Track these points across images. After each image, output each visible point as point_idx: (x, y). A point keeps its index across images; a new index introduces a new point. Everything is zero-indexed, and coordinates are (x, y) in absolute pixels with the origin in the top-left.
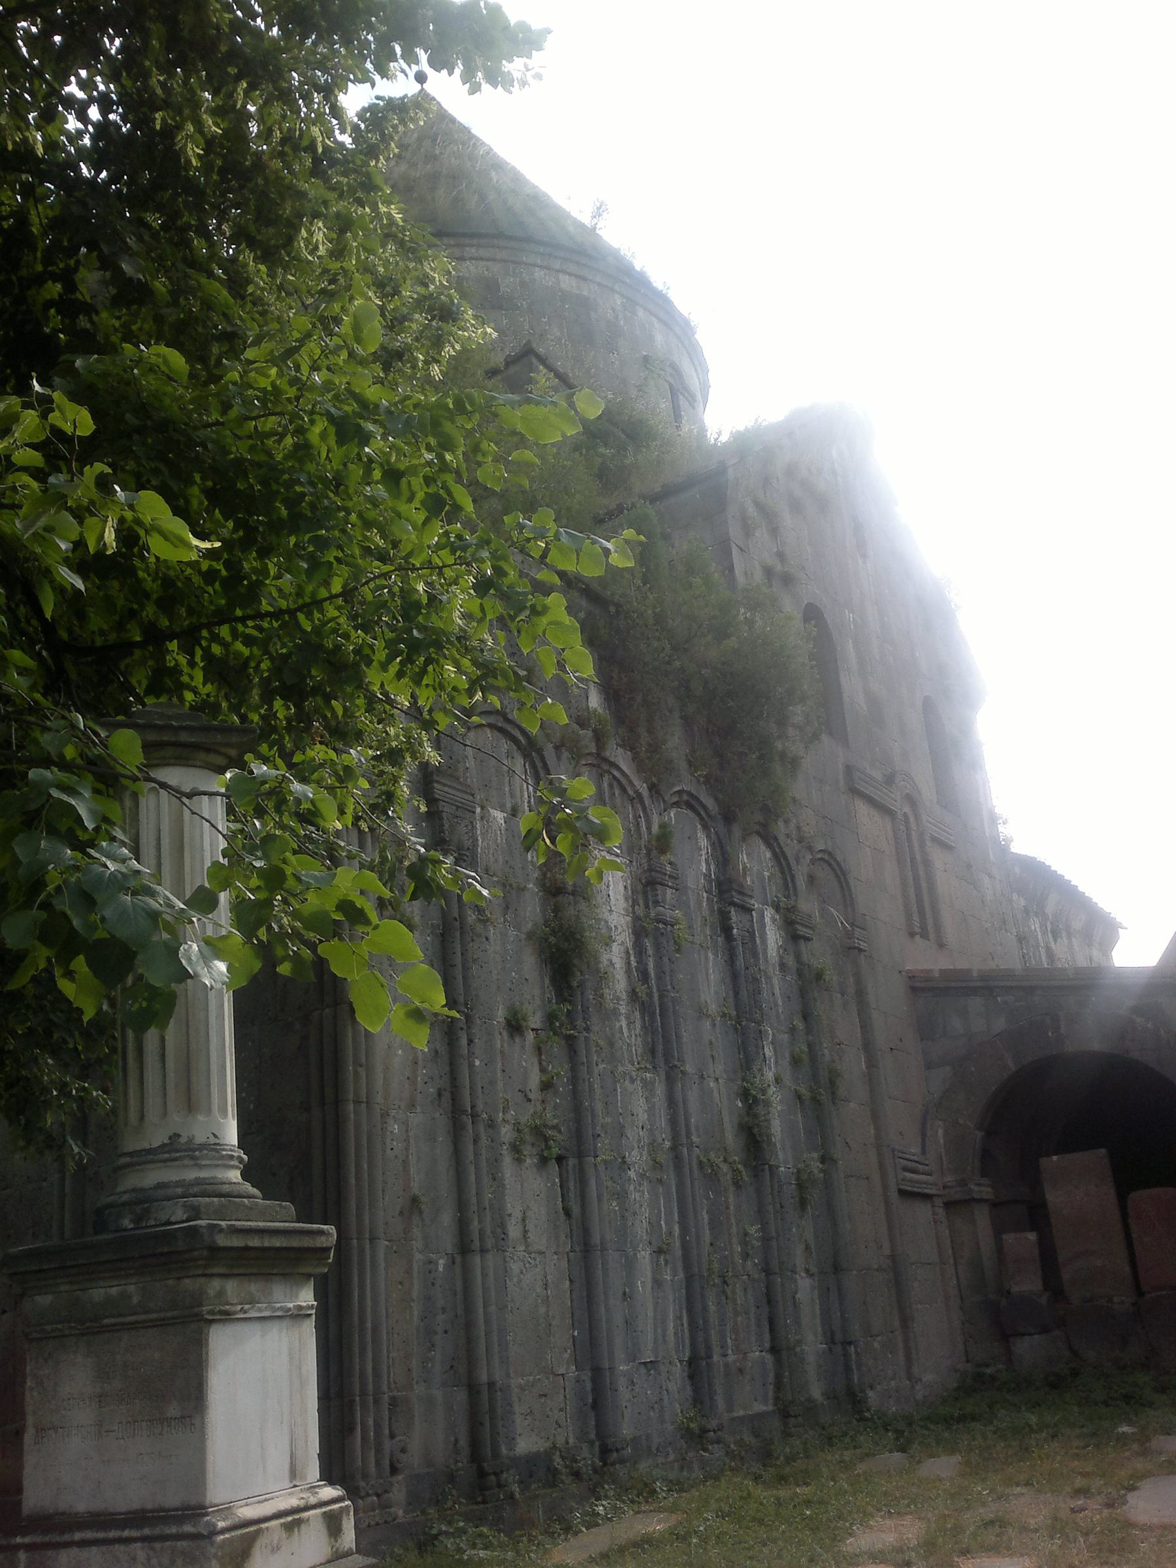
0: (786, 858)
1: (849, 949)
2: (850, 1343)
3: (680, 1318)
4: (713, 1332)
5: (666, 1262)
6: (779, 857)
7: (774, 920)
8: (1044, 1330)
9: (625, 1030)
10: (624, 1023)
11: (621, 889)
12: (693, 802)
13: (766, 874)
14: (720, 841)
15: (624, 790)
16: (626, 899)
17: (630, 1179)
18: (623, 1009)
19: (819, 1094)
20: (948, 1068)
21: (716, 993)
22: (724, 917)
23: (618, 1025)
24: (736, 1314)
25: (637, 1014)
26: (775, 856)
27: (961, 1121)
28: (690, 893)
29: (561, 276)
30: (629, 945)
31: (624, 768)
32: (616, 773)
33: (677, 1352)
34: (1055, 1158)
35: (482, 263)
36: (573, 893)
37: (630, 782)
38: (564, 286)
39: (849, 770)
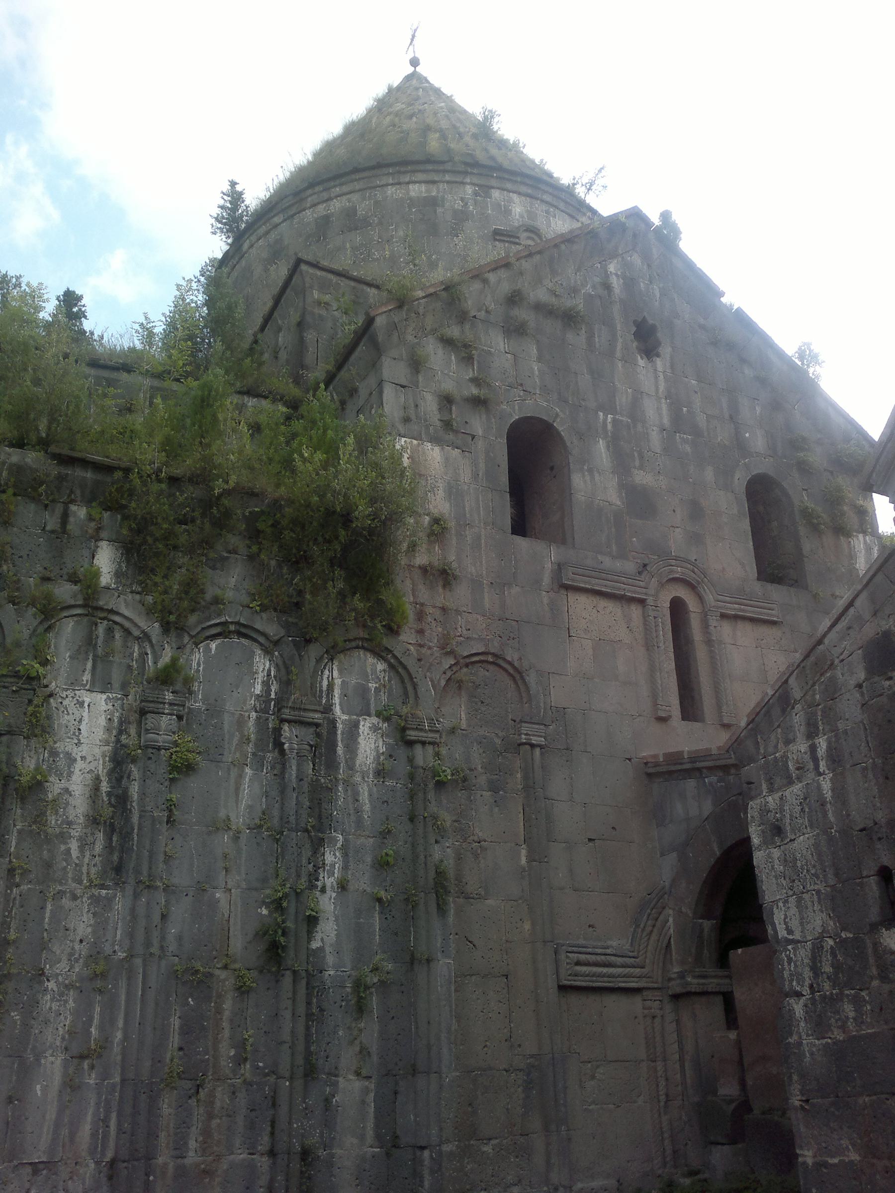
0: (405, 668)
1: (519, 745)
2: (423, 1148)
3: (106, 1121)
4: (163, 1135)
5: (92, 1067)
6: (397, 667)
7: (375, 729)
8: (733, 1141)
9: (75, 853)
10: (74, 846)
11: (102, 721)
12: (243, 630)
13: (372, 686)
14: (284, 662)
15: (127, 632)
16: (108, 730)
17: (46, 990)
18: (76, 832)
19: (416, 894)
20: (675, 855)
21: (250, 807)
22: (277, 731)
23: (63, 847)
24: (210, 1116)
25: (100, 836)
26: (391, 666)
27: (683, 909)
28: (227, 718)
29: (411, 186)
30: (102, 772)
31: (126, 613)
32: (117, 619)
33: (92, 1151)
34: (740, 951)
35: (345, 198)
36: (9, 733)
37: (136, 625)
38: (412, 194)
39: (560, 567)
